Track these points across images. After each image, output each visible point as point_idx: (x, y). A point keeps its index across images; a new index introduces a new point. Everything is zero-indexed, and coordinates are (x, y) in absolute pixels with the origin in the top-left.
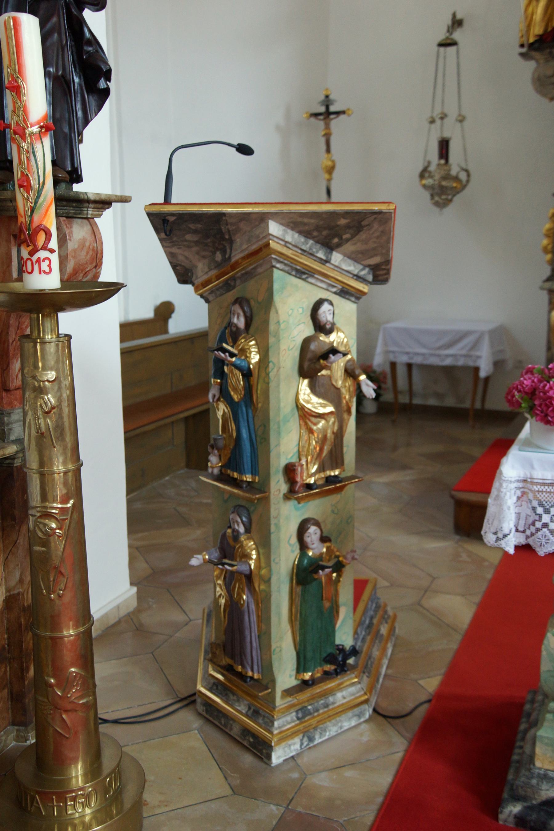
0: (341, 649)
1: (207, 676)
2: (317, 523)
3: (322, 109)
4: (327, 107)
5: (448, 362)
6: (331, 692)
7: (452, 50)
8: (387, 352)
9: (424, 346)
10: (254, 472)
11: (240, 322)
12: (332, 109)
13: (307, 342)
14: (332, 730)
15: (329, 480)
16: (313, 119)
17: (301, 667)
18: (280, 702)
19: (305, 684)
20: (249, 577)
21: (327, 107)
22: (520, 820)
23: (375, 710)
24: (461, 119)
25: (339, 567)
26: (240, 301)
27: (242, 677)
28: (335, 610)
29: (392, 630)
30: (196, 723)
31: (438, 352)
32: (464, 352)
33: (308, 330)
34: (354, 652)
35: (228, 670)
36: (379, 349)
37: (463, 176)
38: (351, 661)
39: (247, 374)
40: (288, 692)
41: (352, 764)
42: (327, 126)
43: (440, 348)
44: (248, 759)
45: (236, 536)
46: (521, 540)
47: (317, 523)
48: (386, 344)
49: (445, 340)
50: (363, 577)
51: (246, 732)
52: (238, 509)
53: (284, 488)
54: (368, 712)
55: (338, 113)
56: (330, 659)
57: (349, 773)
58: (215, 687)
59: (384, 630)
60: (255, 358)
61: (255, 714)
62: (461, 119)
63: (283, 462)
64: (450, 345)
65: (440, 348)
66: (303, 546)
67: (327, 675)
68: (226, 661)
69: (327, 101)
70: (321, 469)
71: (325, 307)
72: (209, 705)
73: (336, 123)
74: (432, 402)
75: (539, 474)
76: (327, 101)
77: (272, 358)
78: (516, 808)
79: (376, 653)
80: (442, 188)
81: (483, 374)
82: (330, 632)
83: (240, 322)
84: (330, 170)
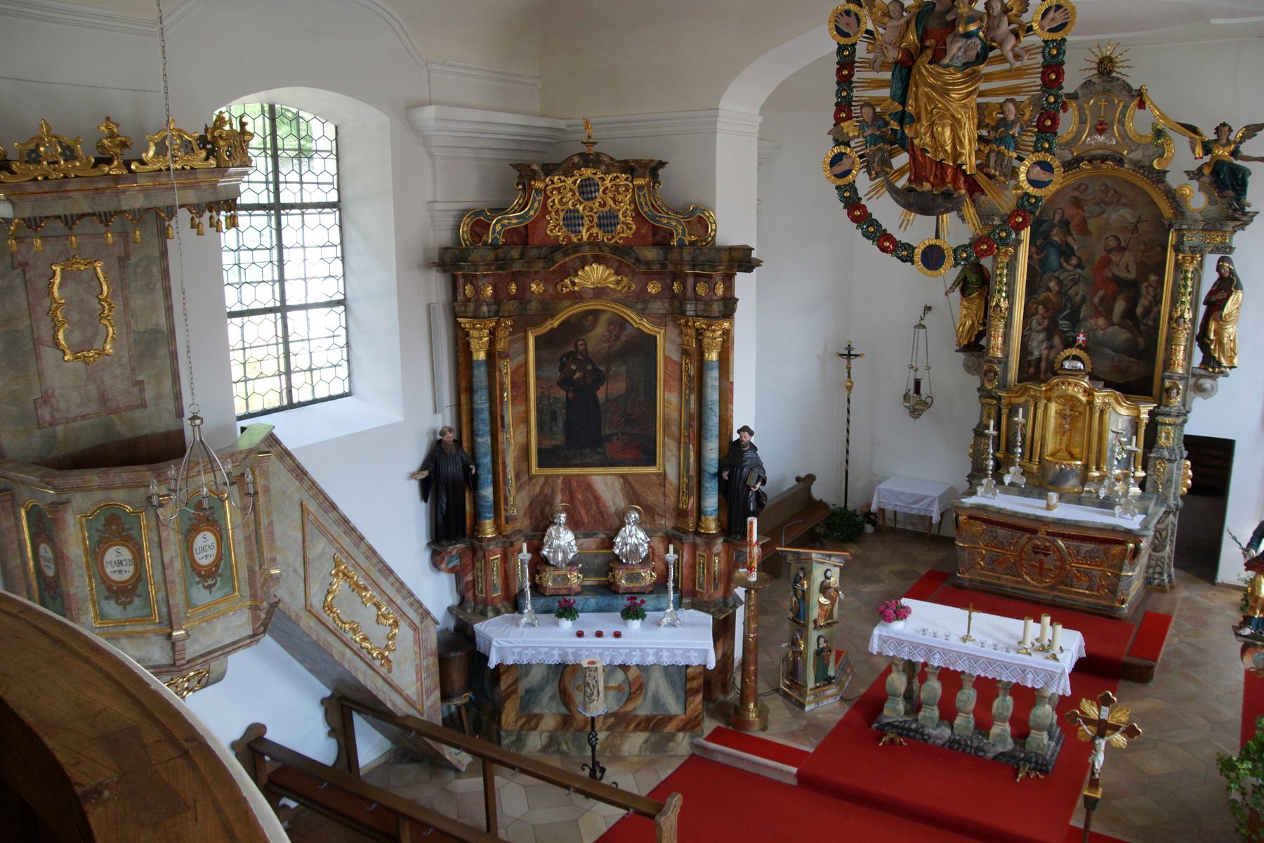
0: (830, 677)
1: (784, 683)
2: (823, 637)
3: (847, 352)
4: (849, 352)
5: (914, 512)
6: (826, 690)
7: (922, 331)
8: (879, 502)
9: (901, 501)
10: (804, 620)
11: (802, 575)
12: (852, 353)
13: (823, 582)
14: (825, 702)
15: (828, 624)
16: (840, 357)
17: (816, 682)
18: (808, 692)
19: (817, 687)
20: (801, 652)
21: (849, 352)
22: (877, 728)
23: (841, 698)
24: (928, 368)
25: (830, 651)
26: (802, 569)
27: (796, 683)
28: (828, 665)
29: (852, 670)
30: (780, 698)
31: (910, 506)
32: (924, 507)
33: (823, 579)
34: (834, 678)
35: (792, 681)
36: (874, 501)
37: (929, 400)
38: (833, 681)
39: (803, 591)
40: (811, 689)
41: (831, 712)
42: (849, 363)
43: (910, 503)
44: (797, 709)
45: (797, 639)
46: (879, 650)
47: (823, 637)
48: (879, 497)
49: (912, 500)
50: (841, 649)
51: (797, 701)
52: (798, 630)
53: (813, 626)
54: (838, 698)
55: (856, 356)
56: (826, 680)
57: (829, 715)
58: (787, 686)
59: (848, 671)
60: (806, 586)
61: (800, 695)
62: (928, 368)
63: (813, 618)
64: (915, 503)
65: (910, 503)
66: (819, 644)
67: (825, 685)
68: (791, 678)
69: (849, 348)
70: (826, 620)
71: (829, 572)
72: (784, 691)
73: (854, 362)
74: (909, 528)
75: (884, 634)
76: (849, 348)
77: (811, 588)
78: (876, 725)
79: (844, 679)
80: (915, 410)
81: (934, 522)
82: (826, 671)
83: (802, 575)
84: (849, 389)
